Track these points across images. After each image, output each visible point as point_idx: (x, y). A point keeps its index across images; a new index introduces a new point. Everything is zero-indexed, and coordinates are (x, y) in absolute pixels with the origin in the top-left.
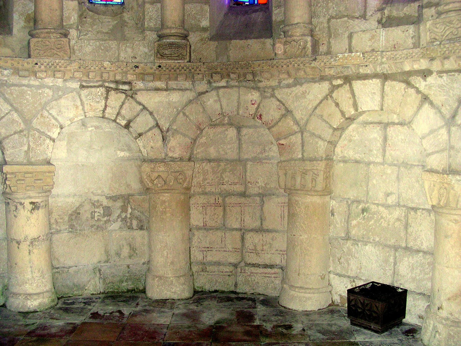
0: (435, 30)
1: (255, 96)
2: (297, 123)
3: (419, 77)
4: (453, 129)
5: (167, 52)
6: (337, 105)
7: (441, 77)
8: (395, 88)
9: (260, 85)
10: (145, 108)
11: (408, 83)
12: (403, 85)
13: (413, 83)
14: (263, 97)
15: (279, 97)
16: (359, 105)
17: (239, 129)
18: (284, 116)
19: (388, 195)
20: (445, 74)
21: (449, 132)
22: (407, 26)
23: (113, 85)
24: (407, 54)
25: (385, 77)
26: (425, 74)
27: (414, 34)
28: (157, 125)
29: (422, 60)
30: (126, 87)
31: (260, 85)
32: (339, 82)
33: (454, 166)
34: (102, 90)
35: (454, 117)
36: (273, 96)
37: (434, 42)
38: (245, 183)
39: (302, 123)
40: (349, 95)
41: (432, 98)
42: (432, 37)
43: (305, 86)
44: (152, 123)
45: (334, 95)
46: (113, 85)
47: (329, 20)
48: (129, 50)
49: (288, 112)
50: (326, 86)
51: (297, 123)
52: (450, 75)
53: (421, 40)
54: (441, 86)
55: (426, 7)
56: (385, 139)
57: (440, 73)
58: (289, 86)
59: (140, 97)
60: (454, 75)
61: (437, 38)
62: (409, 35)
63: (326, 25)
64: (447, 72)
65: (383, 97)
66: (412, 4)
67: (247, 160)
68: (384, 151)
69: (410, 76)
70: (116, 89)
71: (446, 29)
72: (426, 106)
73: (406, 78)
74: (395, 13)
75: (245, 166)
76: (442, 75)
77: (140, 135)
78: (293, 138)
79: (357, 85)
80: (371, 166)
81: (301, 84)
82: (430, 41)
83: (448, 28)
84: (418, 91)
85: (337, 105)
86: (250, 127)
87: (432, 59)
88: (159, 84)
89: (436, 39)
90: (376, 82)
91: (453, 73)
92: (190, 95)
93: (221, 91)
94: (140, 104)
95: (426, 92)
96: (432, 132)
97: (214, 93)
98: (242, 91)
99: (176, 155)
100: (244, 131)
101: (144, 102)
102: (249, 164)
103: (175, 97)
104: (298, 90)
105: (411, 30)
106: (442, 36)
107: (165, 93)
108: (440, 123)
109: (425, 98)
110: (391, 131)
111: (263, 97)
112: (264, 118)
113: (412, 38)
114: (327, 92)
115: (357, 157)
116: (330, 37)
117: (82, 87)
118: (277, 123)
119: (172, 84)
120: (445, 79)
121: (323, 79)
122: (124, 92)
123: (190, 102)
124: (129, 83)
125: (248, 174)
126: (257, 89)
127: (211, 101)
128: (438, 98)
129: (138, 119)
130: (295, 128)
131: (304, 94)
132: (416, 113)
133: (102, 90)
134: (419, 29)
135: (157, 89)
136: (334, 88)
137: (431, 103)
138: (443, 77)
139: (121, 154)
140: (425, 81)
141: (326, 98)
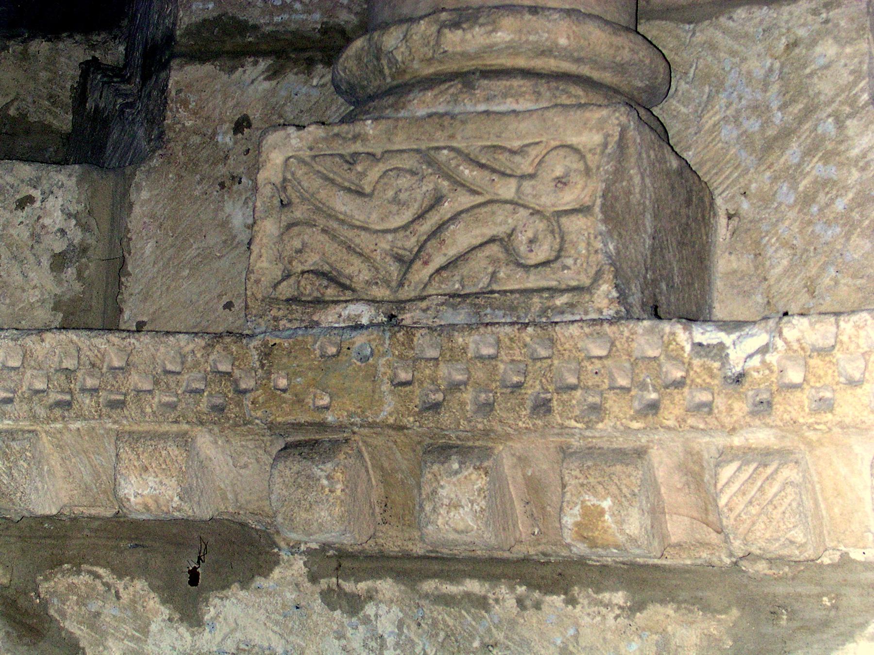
0: (342, 204)
3: (140, 585)
7: (353, 605)
13: (72, 626)
20: (386, 587)
22: (26, 170)
24: (69, 373)
27: (76, 235)
29: (206, 443)
37: (320, 303)
42: (312, 260)
52: (447, 601)
53: (133, 287)
55: (199, 56)
57: (341, 569)
60: (482, 603)
61: (357, 271)
62: (36, 237)
64: (414, 568)
66: (40, 47)
69: (55, 563)
71: (447, 209)
76: (362, 586)
82: (286, 290)
83: (465, 200)
87: (307, 444)
89: (331, 278)
91: (473, 586)
105: (54, 204)
106: (406, 263)
113: (59, 262)
120: (386, 625)
134: (122, 204)
138: (370, 609)
140: (190, 615)
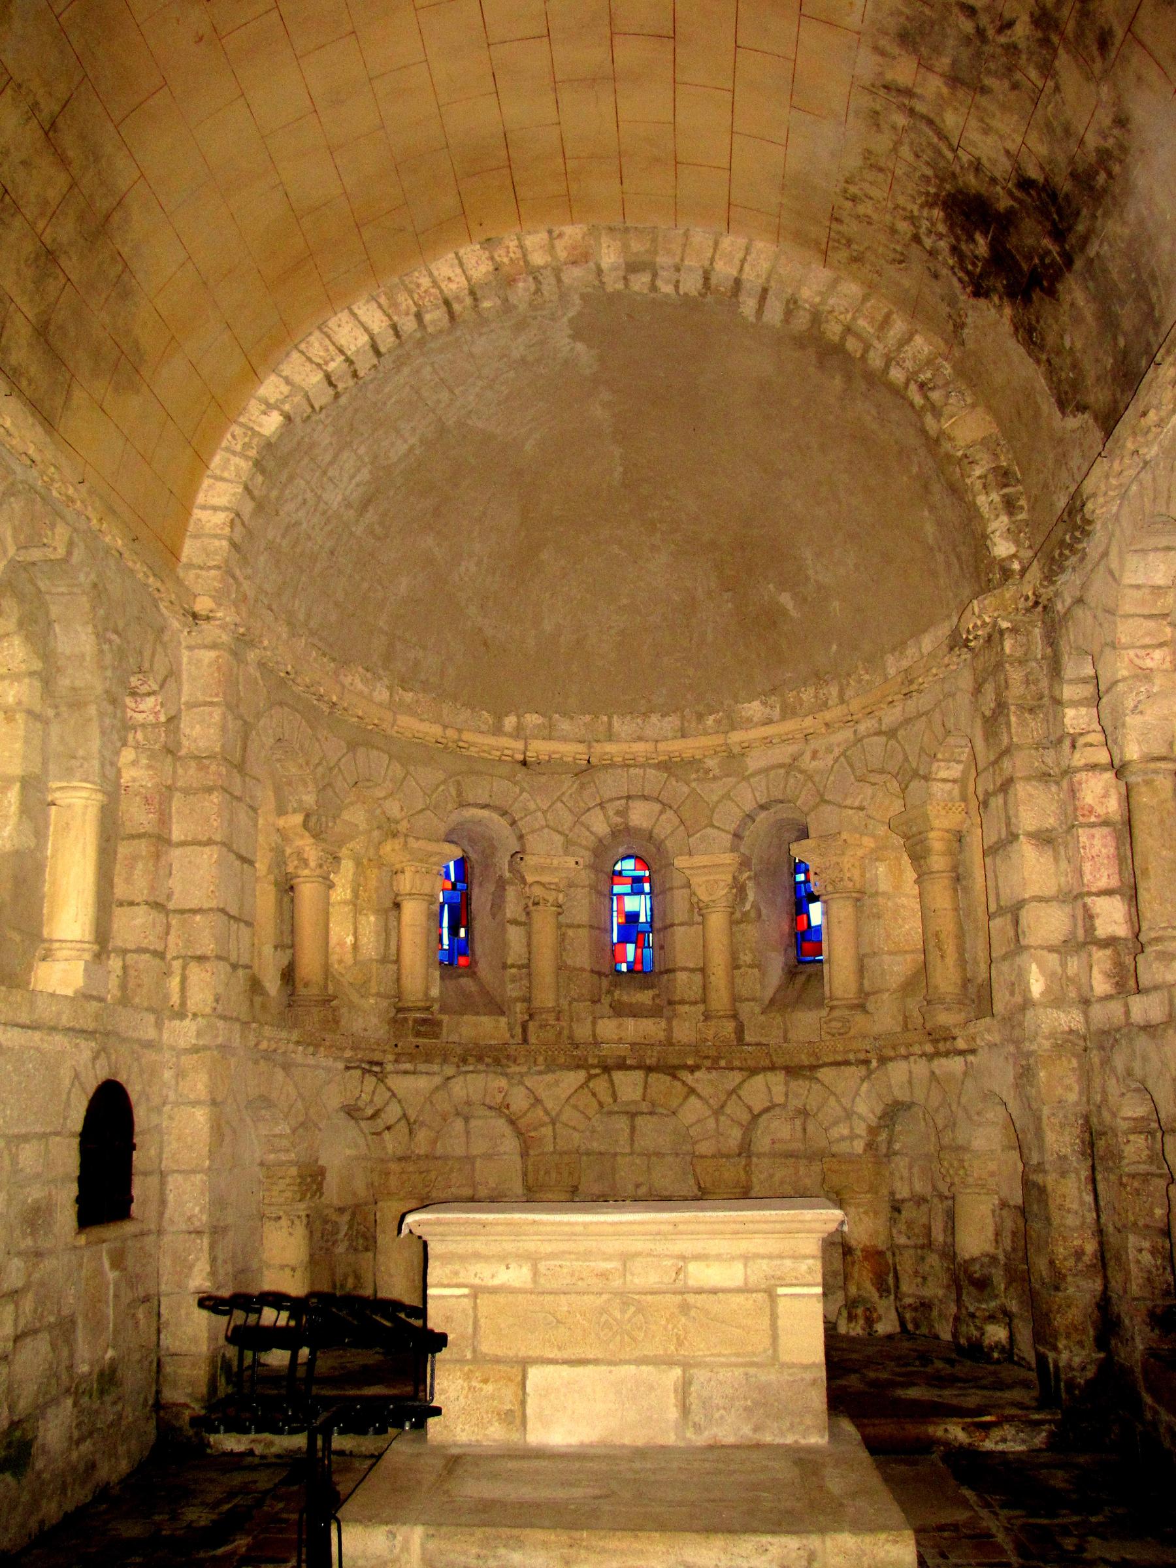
1: (503, 1082)
2: (547, 1112)
4: (722, 1118)
5: (422, 1029)
6: (594, 1095)
8: (660, 1081)
9: (509, 1070)
10: (394, 1095)
11: (675, 1077)
12: (668, 1078)
14: (511, 1085)
15: (528, 1084)
16: (619, 1094)
17: (467, 1120)
18: (533, 1105)
19: (638, 1186)
21: (717, 1120)
23: (367, 1067)
25: (649, 1069)
26: (693, 1069)
28: (405, 1115)
30: (376, 1069)
31: (509, 1070)
32: (597, 1071)
33: (724, 1151)
34: (359, 1072)
35: (722, 1107)
36: (521, 1083)
38: (474, 1186)
39: (553, 1113)
40: (607, 1085)
41: (699, 1090)
43: (558, 1073)
44: (400, 1113)
45: (591, 1085)
46: (367, 1067)
47: (570, 1003)
48: (360, 1020)
49: (538, 1101)
50: (582, 1075)
51: (547, 1112)
54: (710, 1081)
56: (633, 1129)
58: (540, 1073)
59: (392, 1081)
63: (566, 1007)
65: (645, 1088)
67: (475, 1157)
68: (632, 1140)
70: (369, 1071)
72: (693, 1099)
73: (672, 1071)
74: (625, 998)
75: (473, 1164)
77: (388, 1128)
78: (543, 1130)
79: (618, 1076)
80: (619, 1158)
81: (554, 1072)
84: (683, 1082)
85: (594, 1095)
86: (480, 1117)
88: (408, 1066)
90: (639, 1075)
92: (437, 1080)
93: (469, 1076)
94: (389, 1089)
95: (694, 1085)
96: (699, 1121)
97: (461, 1078)
98: (491, 1076)
99: (422, 1152)
100: (473, 1123)
101: (393, 1088)
102: (478, 1161)
103: (422, 1083)
104: (549, 1077)
107: (412, 1077)
108: (708, 1113)
109: (692, 1091)
110: (639, 1121)
111: (511, 1085)
112: (513, 1107)
114: (583, 1080)
115: (602, 1148)
116: (572, 1020)
117: (347, 1068)
118: (525, 1114)
119: (422, 1067)
121: (578, 1067)
122: (375, 1074)
123: (437, 1088)
124: (380, 1064)
125: (477, 1172)
126: (506, 1075)
127: (458, 1088)
128: (705, 1090)
129: (388, 1109)
130: (546, 1119)
131: (557, 1083)
132: (681, 1105)
133: (359, 1072)
135: (406, 1072)
136: (590, 1077)
137: (699, 1096)
139: (348, 1152)
141: (581, 1087)
